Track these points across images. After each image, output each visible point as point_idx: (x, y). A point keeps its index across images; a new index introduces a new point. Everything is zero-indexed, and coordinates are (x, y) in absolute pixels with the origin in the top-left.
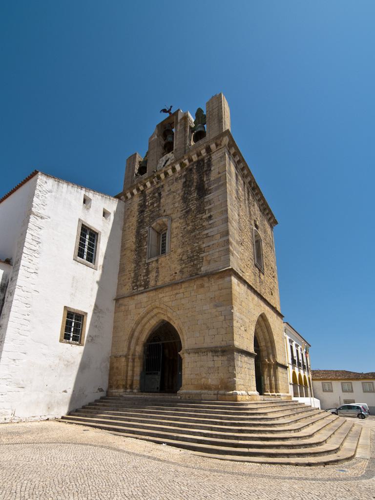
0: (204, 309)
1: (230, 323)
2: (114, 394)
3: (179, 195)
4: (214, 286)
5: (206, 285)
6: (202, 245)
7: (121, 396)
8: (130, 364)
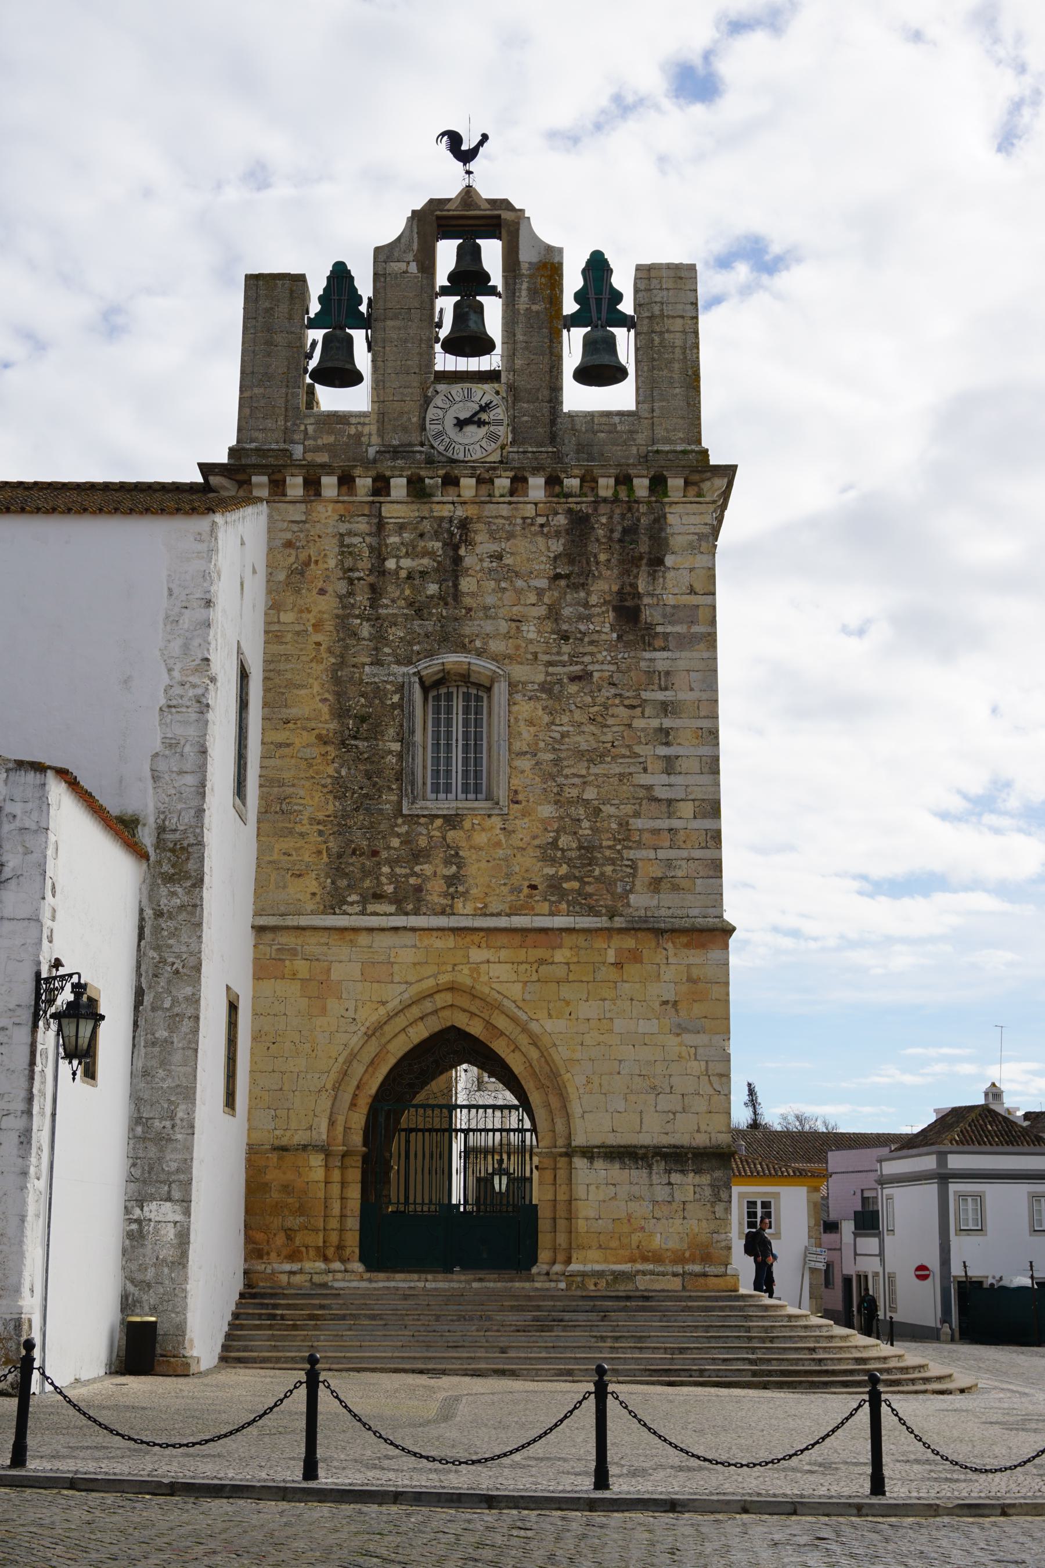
0: (641, 1030)
1: (721, 1084)
2: (284, 1278)
3: (540, 593)
6: (631, 821)
7: (324, 1285)
8: (336, 1175)
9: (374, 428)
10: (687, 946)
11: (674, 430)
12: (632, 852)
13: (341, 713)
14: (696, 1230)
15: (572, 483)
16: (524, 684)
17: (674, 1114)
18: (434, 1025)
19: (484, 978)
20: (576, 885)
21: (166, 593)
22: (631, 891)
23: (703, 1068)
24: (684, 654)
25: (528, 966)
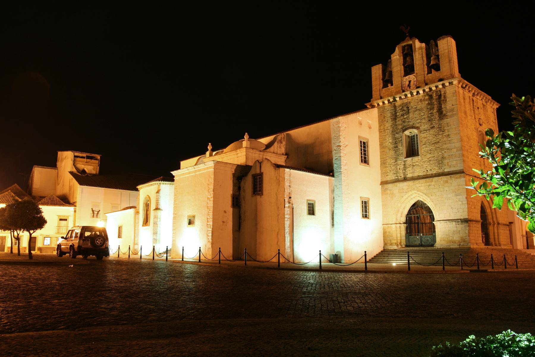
5: (449, 181)
7: (396, 250)
9: (394, 89)
14: (462, 236)
22: (445, 169)
24: (453, 118)
25: (427, 187)
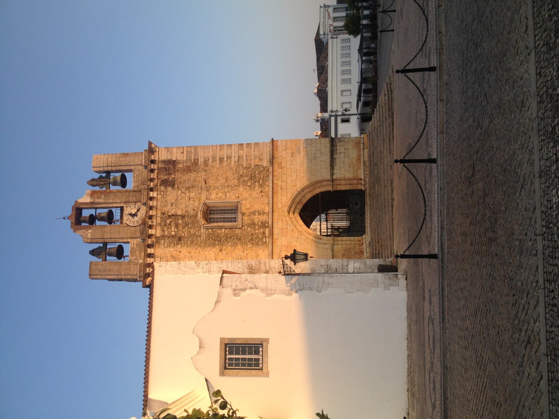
0: (299, 162)
3: (183, 193)
4: (281, 153)
6: (244, 167)
7: (370, 243)
9: (135, 240)
10: (277, 152)
11: (139, 159)
12: (252, 166)
13: (214, 245)
15: (152, 185)
16: (207, 196)
17: (321, 153)
18: (299, 218)
19: (286, 204)
20: (261, 180)
21: (176, 275)
22: (263, 166)
23: (309, 146)
24: (200, 154)
